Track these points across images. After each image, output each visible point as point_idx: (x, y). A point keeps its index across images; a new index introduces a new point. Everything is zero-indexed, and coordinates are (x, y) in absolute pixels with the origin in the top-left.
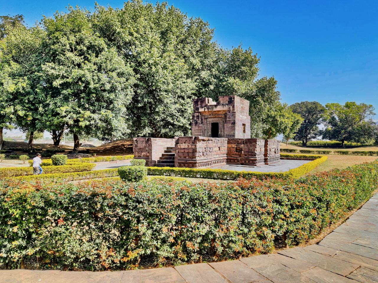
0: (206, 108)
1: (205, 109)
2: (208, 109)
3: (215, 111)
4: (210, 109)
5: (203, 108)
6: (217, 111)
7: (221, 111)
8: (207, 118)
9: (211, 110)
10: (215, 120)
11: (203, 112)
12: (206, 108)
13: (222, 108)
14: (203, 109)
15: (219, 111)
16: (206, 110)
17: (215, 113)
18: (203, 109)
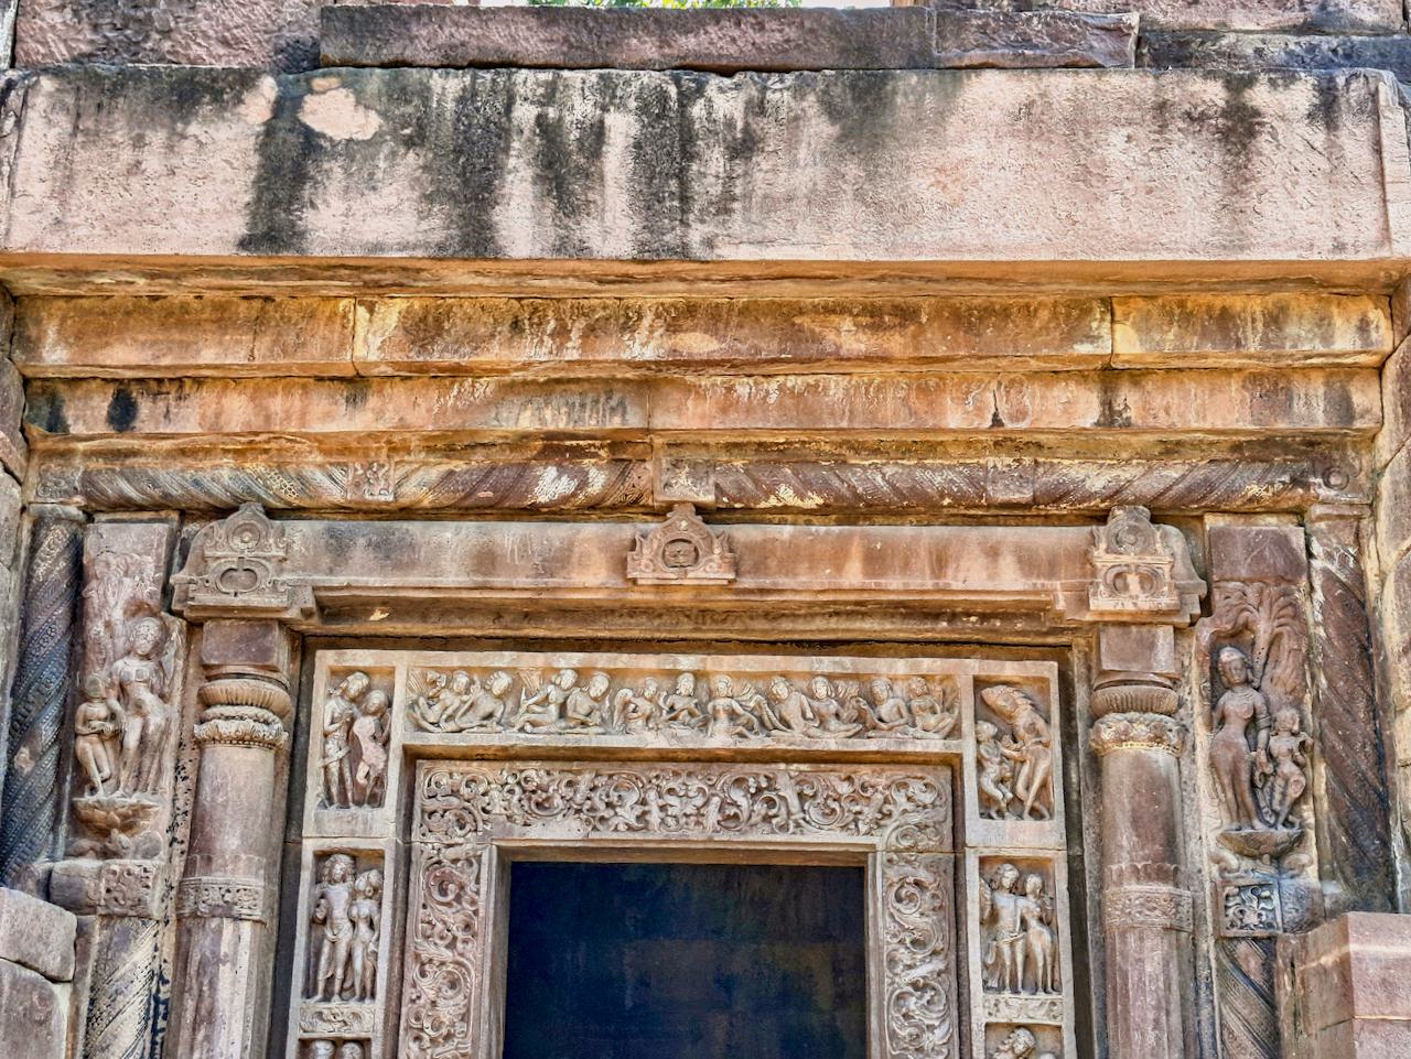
0: (335, 111)
1: (290, 162)
2: (468, 185)
3: (782, 318)
4: (564, 171)
5: (192, 93)
6: (901, 302)
7: (1097, 292)
8: (333, 622)
9: (613, 227)
10: (669, 759)
11: (165, 295)
12: (335, 111)
13: (1192, 161)
14: (227, 145)
15: (965, 308)
16: (372, 211)
17: (762, 404)
18: (227, 145)
